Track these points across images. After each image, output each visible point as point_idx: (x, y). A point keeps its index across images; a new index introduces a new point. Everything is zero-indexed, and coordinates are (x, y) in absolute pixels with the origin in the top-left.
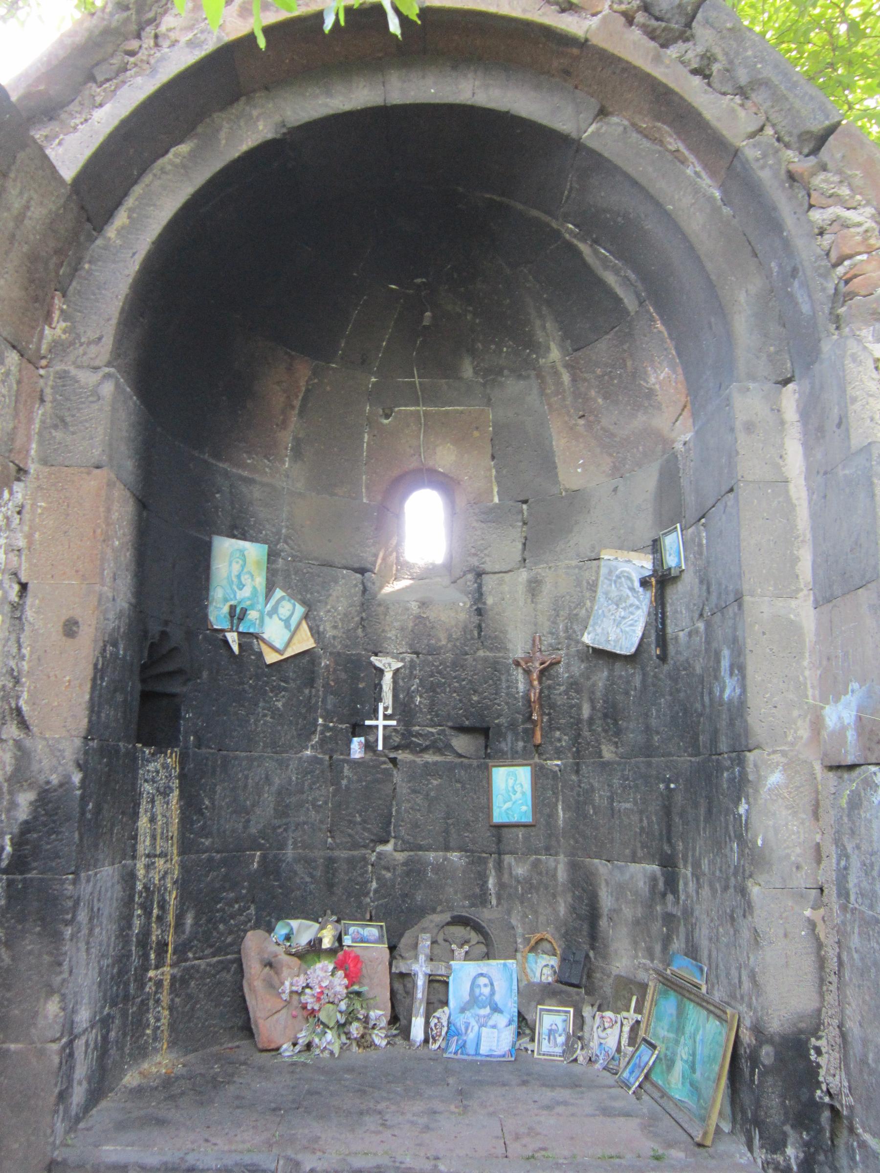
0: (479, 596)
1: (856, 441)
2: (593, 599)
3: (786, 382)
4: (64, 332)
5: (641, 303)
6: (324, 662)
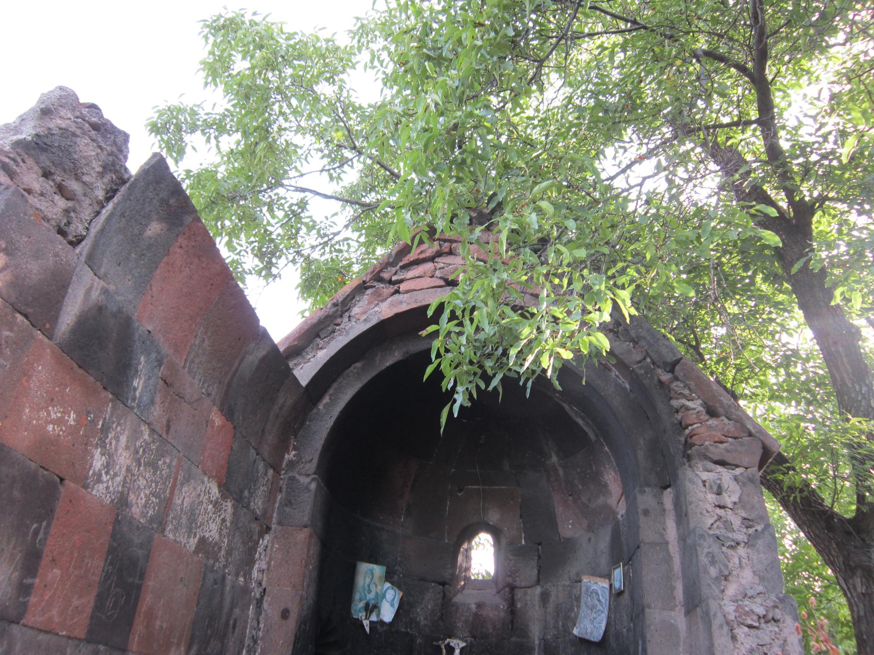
0: (512, 602)
1: (692, 526)
2: (579, 607)
3: (666, 487)
4: (294, 456)
5: (597, 436)
6: (419, 641)
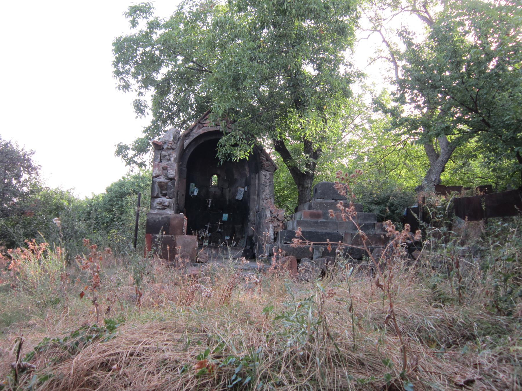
0: (222, 191)
